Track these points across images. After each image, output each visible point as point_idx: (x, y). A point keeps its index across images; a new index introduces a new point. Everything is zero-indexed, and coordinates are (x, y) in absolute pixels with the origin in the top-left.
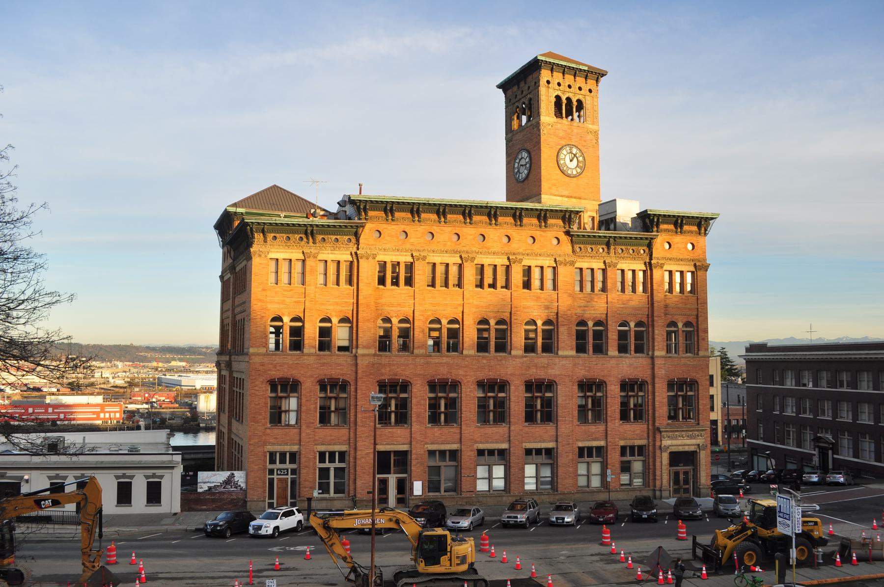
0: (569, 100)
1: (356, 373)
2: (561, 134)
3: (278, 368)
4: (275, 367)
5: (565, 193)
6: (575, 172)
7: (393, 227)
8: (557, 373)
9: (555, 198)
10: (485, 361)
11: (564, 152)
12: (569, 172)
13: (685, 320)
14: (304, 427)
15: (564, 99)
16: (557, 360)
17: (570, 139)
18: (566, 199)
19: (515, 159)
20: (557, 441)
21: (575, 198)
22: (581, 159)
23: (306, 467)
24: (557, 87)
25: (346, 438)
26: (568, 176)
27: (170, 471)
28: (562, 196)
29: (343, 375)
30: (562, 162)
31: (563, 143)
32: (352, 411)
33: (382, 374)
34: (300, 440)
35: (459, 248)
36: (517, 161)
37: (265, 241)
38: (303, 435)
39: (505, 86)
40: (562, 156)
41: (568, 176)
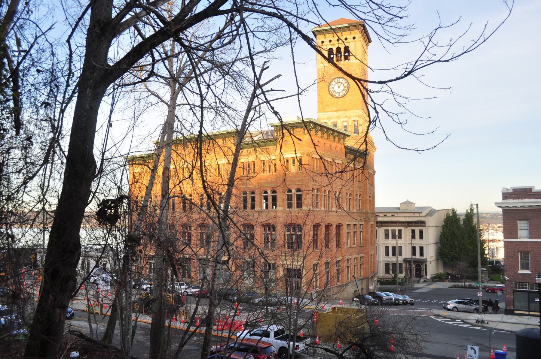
0: (338, 49)
5: (335, 109)
6: (341, 94)
9: (327, 113)
11: (333, 83)
12: (337, 95)
13: (296, 187)
15: (334, 49)
18: (335, 113)
21: (341, 110)
22: (346, 85)
24: (329, 43)
26: (337, 98)
28: (332, 111)
30: (331, 90)
31: (334, 77)
40: (331, 86)
41: (337, 98)
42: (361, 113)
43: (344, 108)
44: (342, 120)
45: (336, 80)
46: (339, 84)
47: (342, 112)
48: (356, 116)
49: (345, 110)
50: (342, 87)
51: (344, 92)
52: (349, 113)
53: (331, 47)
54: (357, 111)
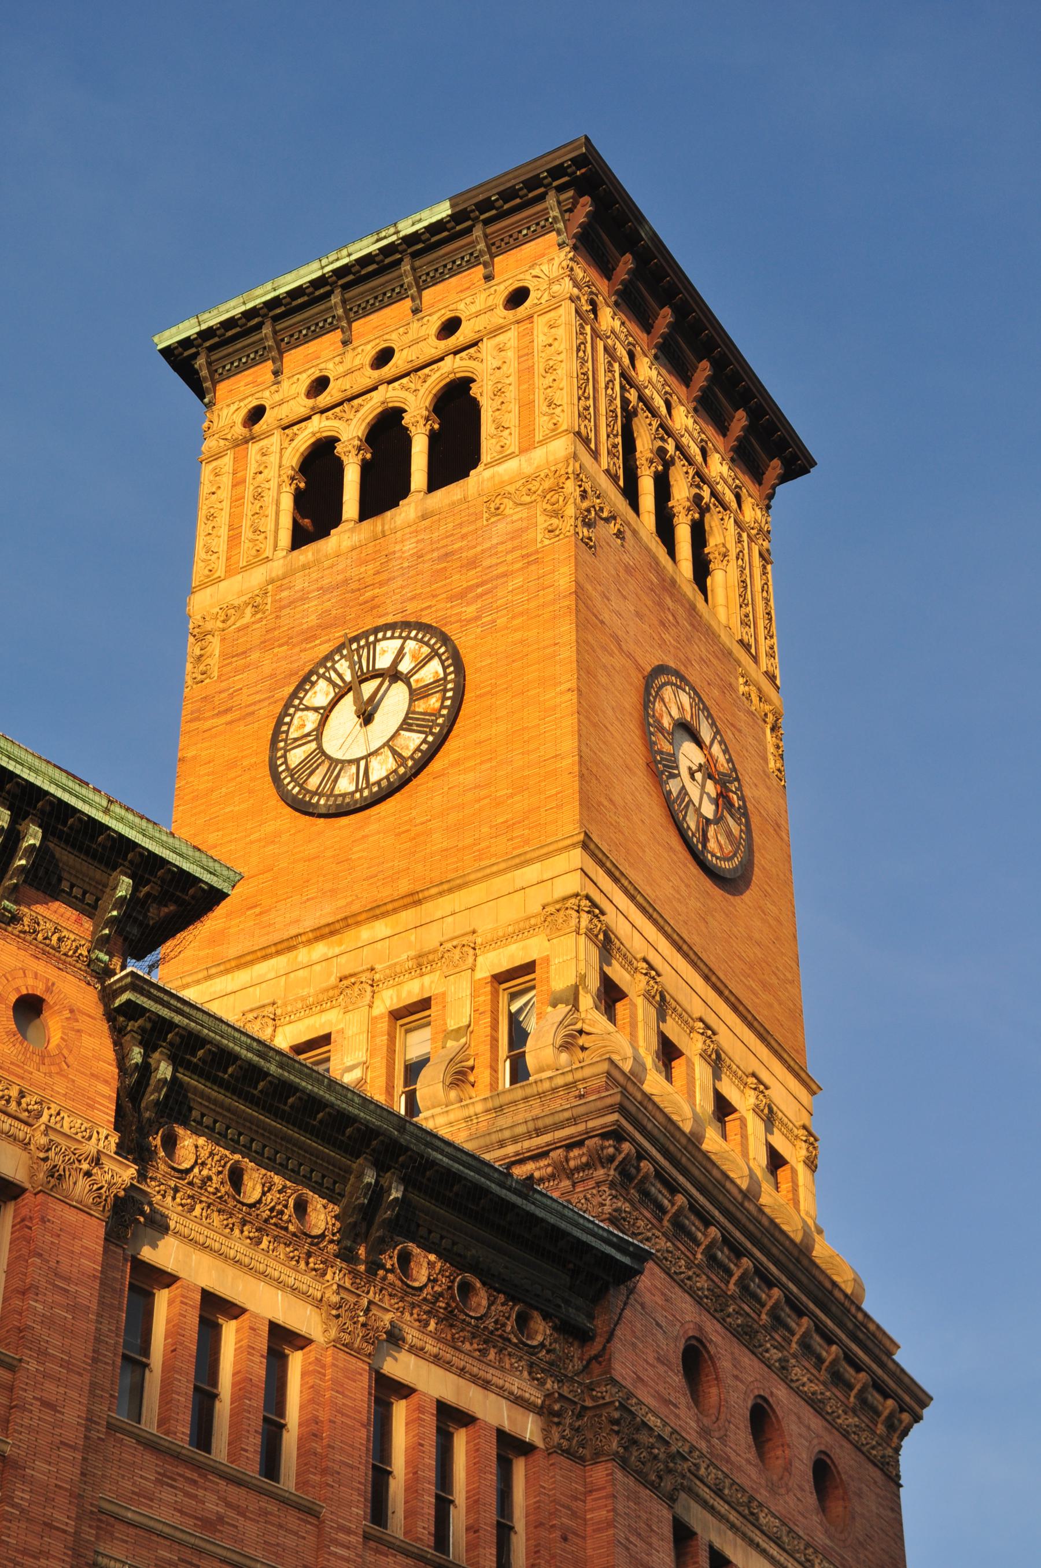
2: (310, 614)
6: (381, 769)
11: (320, 694)
12: (345, 785)
17: (372, 606)
18: (320, 950)
21: (376, 912)
31: (324, 649)
42: (573, 883)
43: (404, 886)
44: (389, 999)
45: (343, 666)
46: (368, 688)
47: (381, 928)
48: (523, 930)
49: (414, 900)
50: (395, 701)
51: (412, 742)
52: (445, 917)
53: (319, 426)
54: (531, 873)
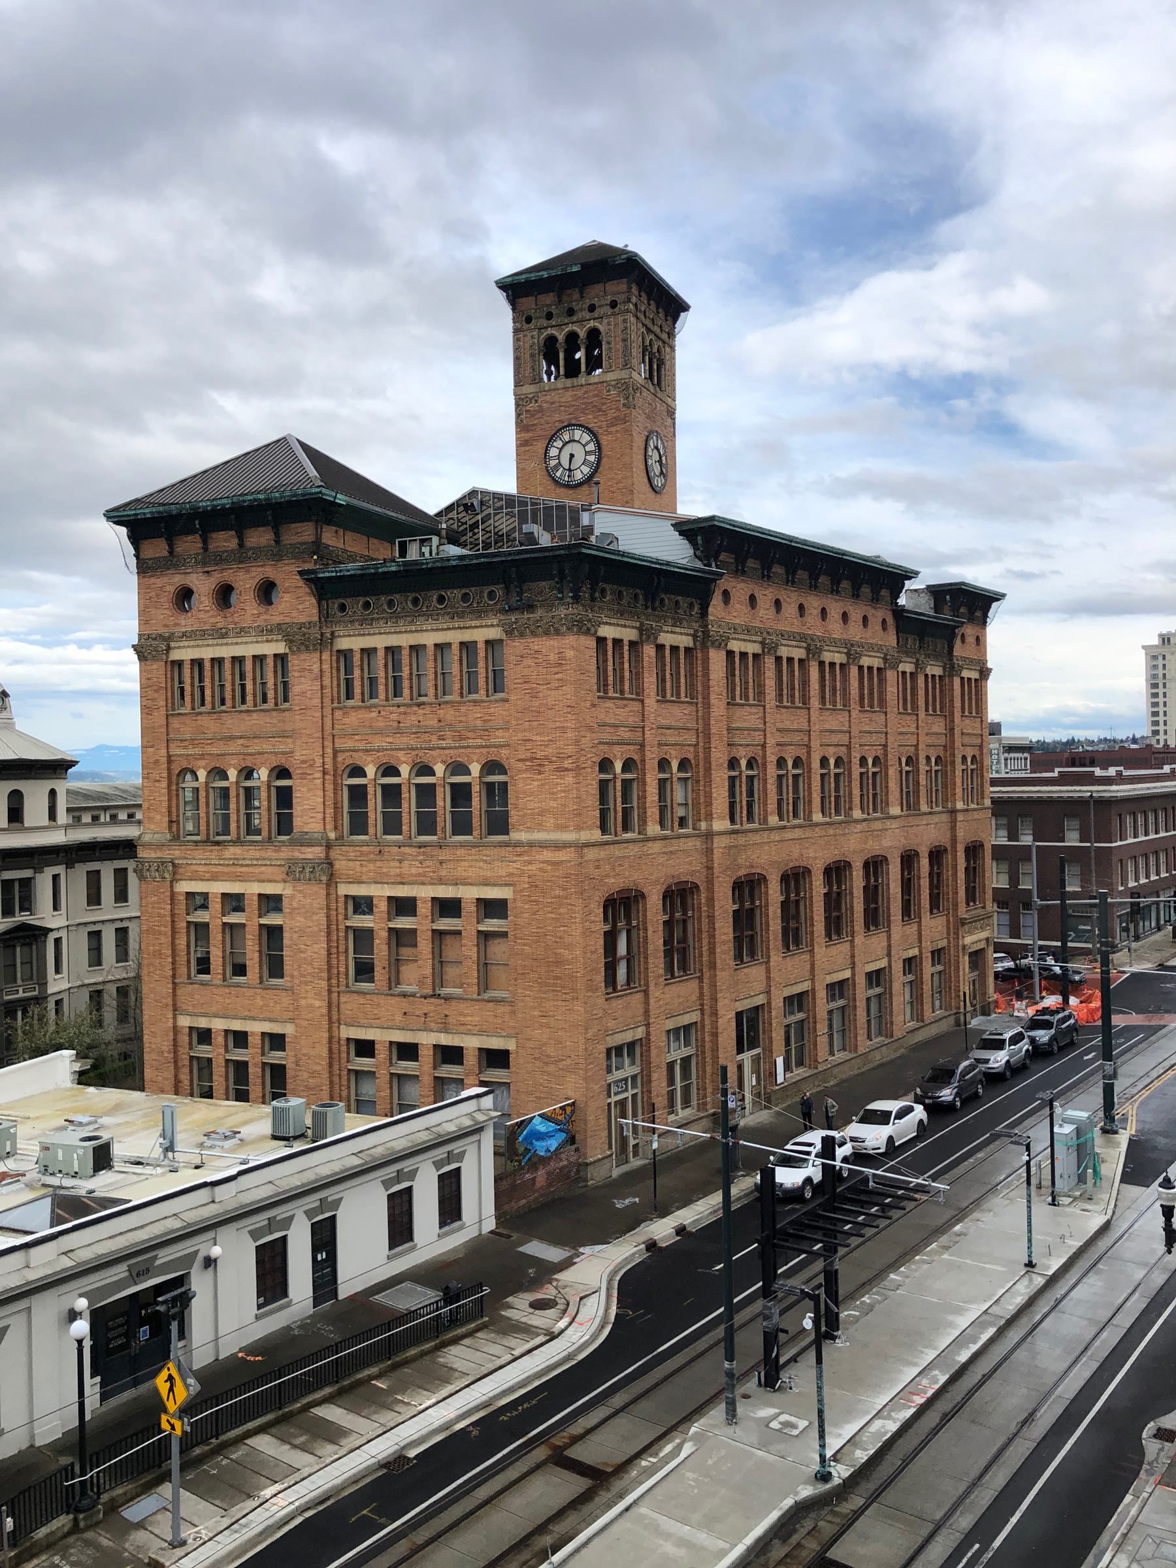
1: (710, 868)
3: (618, 869)
4: (613, 869)
7: (742, 585)
8: (889, 844)
10: (831, 832)
14: (652, 987)
16: (888, 823)
19: (552, 439)
20: (889, 955)
23: (658, 1067)
25: (694, 997)
27: (475, 1138)
29: (692, 873)
32: (705, 942)
33: (739, 867)
34: (647, 1012)
35: (804, 630)
36: (559, 444)
37: (593, 599)
38: (652, 1001)
39: (517, 289)
